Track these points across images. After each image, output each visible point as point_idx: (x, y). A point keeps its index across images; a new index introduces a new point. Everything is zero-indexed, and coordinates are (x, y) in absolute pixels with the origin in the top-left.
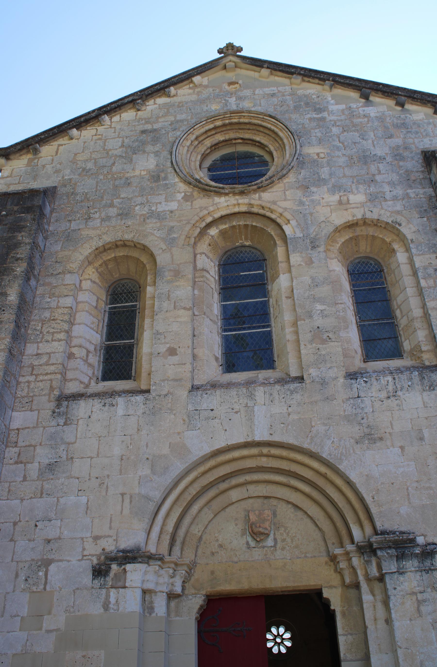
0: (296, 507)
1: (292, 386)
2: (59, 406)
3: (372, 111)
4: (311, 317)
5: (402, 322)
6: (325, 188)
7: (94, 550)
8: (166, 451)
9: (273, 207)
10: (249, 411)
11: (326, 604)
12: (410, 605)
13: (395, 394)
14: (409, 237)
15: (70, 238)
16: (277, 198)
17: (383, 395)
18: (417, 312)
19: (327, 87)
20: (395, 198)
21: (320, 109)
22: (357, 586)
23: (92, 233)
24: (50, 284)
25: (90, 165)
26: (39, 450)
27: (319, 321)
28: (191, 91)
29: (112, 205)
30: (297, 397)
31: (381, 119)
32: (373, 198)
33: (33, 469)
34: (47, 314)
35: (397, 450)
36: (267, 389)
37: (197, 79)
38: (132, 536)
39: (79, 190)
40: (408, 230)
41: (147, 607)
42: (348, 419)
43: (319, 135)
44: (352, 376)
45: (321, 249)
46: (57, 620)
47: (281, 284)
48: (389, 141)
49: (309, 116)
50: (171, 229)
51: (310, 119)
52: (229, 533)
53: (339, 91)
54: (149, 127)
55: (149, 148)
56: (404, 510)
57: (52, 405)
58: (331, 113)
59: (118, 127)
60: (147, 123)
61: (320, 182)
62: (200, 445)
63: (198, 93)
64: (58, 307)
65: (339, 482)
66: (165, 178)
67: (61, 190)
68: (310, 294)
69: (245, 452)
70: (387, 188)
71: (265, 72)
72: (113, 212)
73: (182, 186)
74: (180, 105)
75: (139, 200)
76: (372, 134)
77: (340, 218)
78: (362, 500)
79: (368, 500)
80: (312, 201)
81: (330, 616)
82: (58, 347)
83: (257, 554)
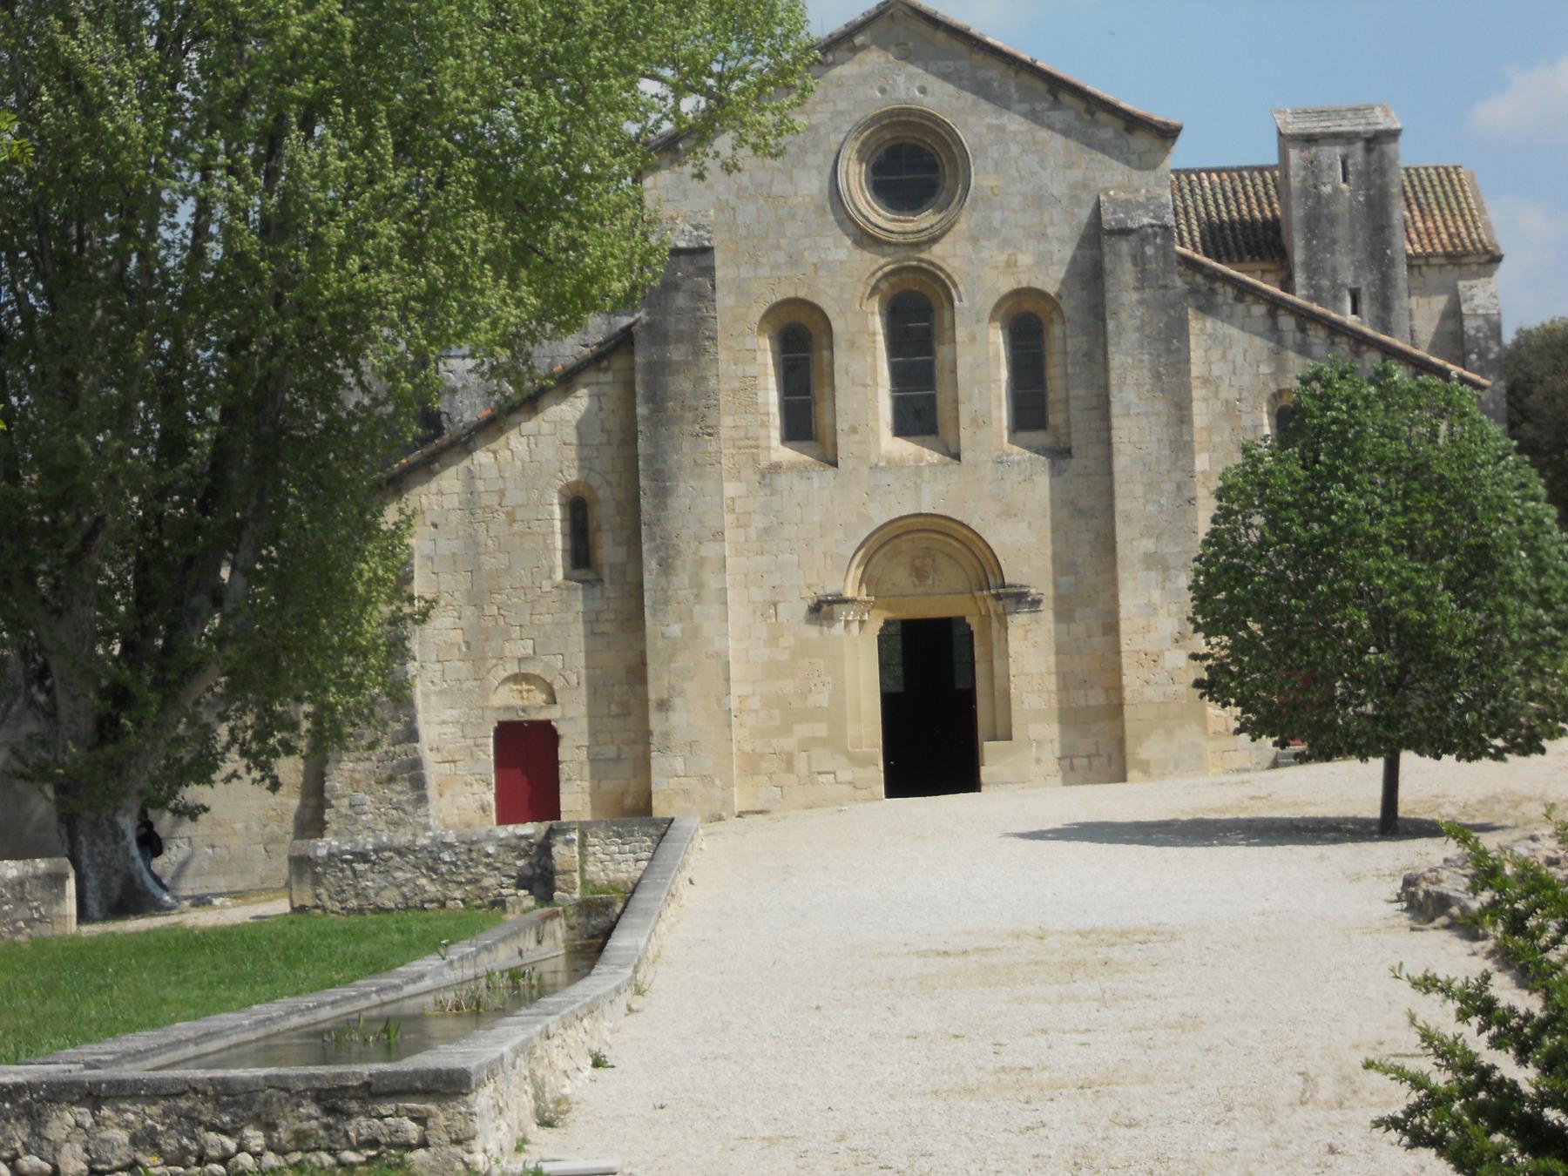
0: (950, 556)
5: (1051, 396)
6: (995, 241)
10: (917, 488)
12: (1021, 632)
14: (1067, 314)
17: (1021, 479)
19: (1012, 73)
29: (778, 247)
33: (752, 532)
35: (1025, 525)
40: (1067, 306)
43: (996, 155)
46: (788, 641)
48: (1068, 172)
49: (987, 121)
51: (990, 127)
53: (1025, 78)
55: (811, 159)
56: (1026, 569)
57: (758, 477)
61: (992, 232)
62: (880, 517)
70: (1055, 247)
71: (941, 36)
72: (781, 257)
75: (807, 242)
77: (1007, 285)
81: (971, 634)
83: (920, 590)
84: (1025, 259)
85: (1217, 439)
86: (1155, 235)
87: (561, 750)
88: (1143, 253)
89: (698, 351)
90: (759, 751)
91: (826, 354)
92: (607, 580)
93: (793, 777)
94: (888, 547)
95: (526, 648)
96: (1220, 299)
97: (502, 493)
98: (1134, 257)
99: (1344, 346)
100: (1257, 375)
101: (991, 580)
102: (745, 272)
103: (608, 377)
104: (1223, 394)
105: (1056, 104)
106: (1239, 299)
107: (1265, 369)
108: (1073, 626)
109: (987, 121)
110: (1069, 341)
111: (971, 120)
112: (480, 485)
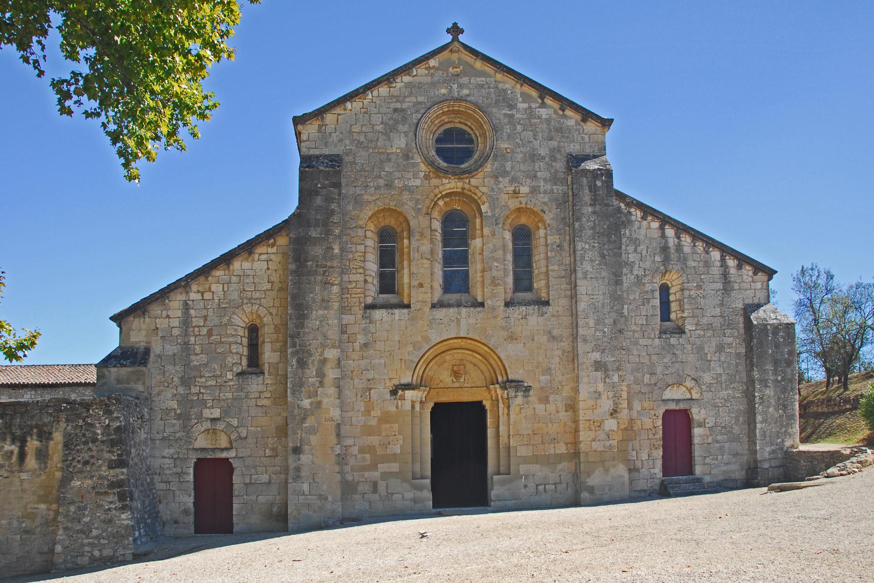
1: (479, 309)
2: (365, 313)
3: (543, 112)
4: (491, 270)
6: (507, 179)
7: (390, 385)
8: (420, 339)
9: (477, 191)
10: (458, 320)
11: (484, 407)
12: (517, 409)
13: (525, 317)
14: (548, 222)
15: (358, 201)
16: (480, 182)
17: (520, 317)
18: (544, 269)
20: (545, 192)
21: (511, 105)
22: (498, 400)
23: (370, 198)
24: (349, 235)
25: (362, 139)
26: (358, 336)
27: (495, 273)
28: (427, 72)
29: (380, 177)
30: (481, 315)
31: (548, 121)
32: (534, 191)
33: (357, 346)
34: (351, 256)
35: (522, 345)
36: (468, 309)
37: (432, 62)
38: (406, 379)
39: (357, 160)
40: (548, 218)
41: (413, 407)
42: (503, 328)
43: (508, 131)
44: (507, 304)
45: (500, 226)
46: (377, 413)
47: (476, 243)
48: (550, 142)
49: (504, 111)
50: (417, 201)
51: (505, 115)
52: (446, 378)
53: (527, 89)
54: (398, 105)
55: (400, 127)
57: (361, 312)
58: (518, 111)
59: (378, 102)
60: (397, 101)
61: (505, 173)
63: (432, 75)
64: (357, 252)
65: (495, 357)
66: (413, 158)
67: (347, 159)
68: (490, 248)
69: (455, 341)
70: (542, 183)
72: (381, 182)
73: (423, 167)
74: (420, 85)
75: (397, 174)
76: (540, 134)
77: (513, 204)
78: (504, 366)
79: (507, 366)
80: (499, 189)
82: (361, 278)
84: (524, 190)
85: (631, 297)
86: (602, 175)
87: (234, 477)
88: (595, 185)
89: (328, 233)
90: (356, 480)
91: (406, 241)
92: (266, 373)
93: (377, 496)
94: (438, 358)
95: (216, 413)
96: (633, 218)
97: (205, 318)
98: (590, 187)
99: (700, 246)
100: (654, 261)
101: (500, 379)
102: (358, 191)
103: (274, 250)
104: (635, 273)
105: (543, 105)
106: (644, 218)
107: (658, 259)
108: (548, 405)
109: (504, 111)
110: (548, 237)
111: (495, 110)
112: (192, 312)
